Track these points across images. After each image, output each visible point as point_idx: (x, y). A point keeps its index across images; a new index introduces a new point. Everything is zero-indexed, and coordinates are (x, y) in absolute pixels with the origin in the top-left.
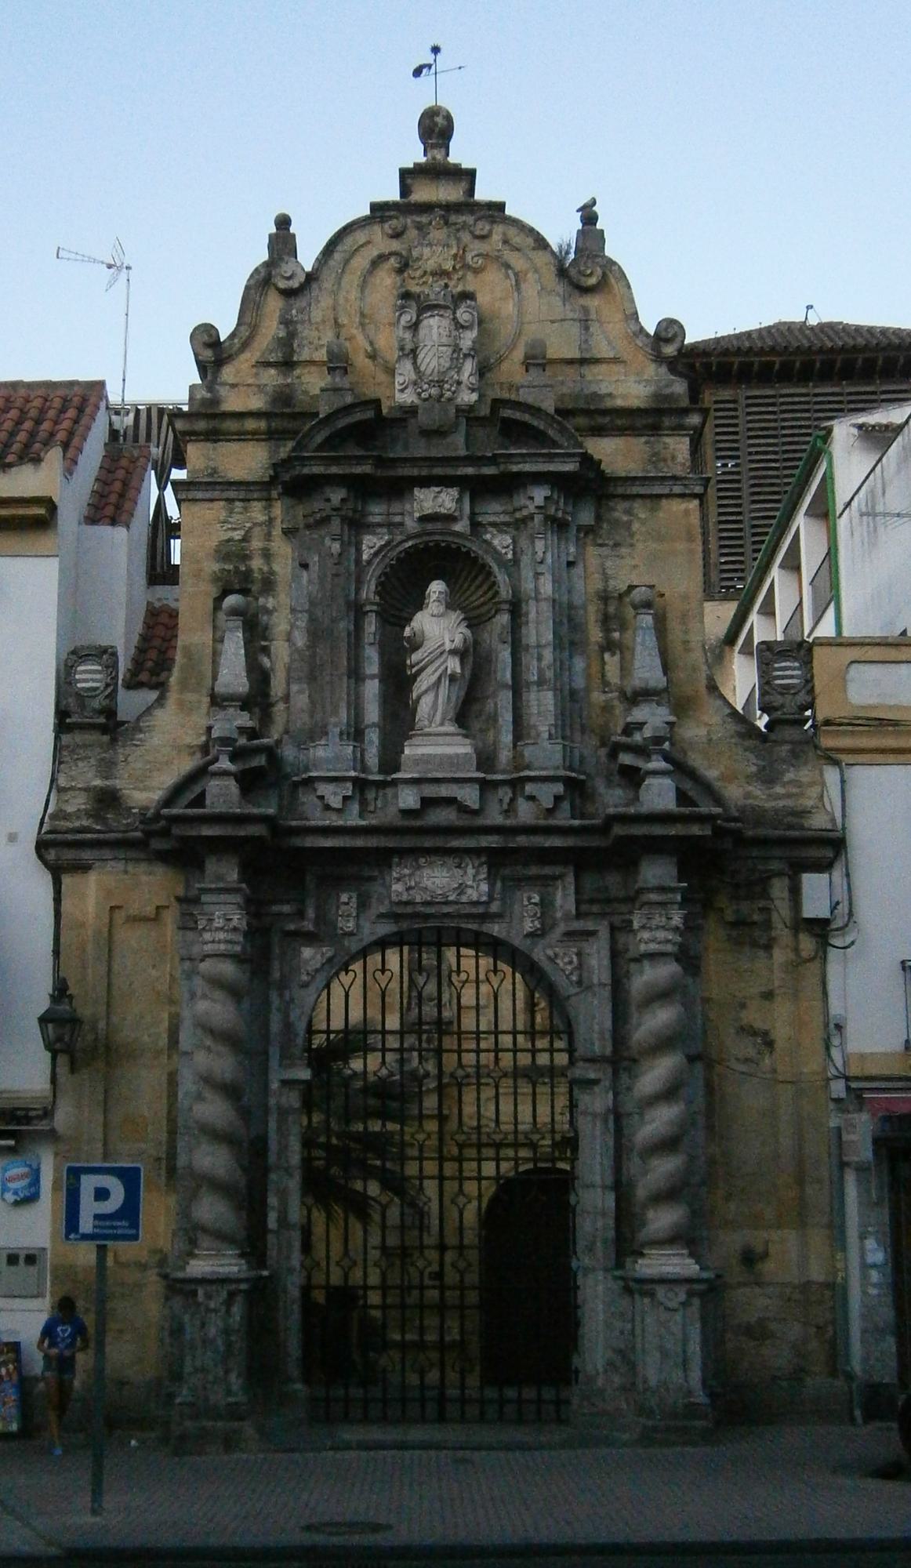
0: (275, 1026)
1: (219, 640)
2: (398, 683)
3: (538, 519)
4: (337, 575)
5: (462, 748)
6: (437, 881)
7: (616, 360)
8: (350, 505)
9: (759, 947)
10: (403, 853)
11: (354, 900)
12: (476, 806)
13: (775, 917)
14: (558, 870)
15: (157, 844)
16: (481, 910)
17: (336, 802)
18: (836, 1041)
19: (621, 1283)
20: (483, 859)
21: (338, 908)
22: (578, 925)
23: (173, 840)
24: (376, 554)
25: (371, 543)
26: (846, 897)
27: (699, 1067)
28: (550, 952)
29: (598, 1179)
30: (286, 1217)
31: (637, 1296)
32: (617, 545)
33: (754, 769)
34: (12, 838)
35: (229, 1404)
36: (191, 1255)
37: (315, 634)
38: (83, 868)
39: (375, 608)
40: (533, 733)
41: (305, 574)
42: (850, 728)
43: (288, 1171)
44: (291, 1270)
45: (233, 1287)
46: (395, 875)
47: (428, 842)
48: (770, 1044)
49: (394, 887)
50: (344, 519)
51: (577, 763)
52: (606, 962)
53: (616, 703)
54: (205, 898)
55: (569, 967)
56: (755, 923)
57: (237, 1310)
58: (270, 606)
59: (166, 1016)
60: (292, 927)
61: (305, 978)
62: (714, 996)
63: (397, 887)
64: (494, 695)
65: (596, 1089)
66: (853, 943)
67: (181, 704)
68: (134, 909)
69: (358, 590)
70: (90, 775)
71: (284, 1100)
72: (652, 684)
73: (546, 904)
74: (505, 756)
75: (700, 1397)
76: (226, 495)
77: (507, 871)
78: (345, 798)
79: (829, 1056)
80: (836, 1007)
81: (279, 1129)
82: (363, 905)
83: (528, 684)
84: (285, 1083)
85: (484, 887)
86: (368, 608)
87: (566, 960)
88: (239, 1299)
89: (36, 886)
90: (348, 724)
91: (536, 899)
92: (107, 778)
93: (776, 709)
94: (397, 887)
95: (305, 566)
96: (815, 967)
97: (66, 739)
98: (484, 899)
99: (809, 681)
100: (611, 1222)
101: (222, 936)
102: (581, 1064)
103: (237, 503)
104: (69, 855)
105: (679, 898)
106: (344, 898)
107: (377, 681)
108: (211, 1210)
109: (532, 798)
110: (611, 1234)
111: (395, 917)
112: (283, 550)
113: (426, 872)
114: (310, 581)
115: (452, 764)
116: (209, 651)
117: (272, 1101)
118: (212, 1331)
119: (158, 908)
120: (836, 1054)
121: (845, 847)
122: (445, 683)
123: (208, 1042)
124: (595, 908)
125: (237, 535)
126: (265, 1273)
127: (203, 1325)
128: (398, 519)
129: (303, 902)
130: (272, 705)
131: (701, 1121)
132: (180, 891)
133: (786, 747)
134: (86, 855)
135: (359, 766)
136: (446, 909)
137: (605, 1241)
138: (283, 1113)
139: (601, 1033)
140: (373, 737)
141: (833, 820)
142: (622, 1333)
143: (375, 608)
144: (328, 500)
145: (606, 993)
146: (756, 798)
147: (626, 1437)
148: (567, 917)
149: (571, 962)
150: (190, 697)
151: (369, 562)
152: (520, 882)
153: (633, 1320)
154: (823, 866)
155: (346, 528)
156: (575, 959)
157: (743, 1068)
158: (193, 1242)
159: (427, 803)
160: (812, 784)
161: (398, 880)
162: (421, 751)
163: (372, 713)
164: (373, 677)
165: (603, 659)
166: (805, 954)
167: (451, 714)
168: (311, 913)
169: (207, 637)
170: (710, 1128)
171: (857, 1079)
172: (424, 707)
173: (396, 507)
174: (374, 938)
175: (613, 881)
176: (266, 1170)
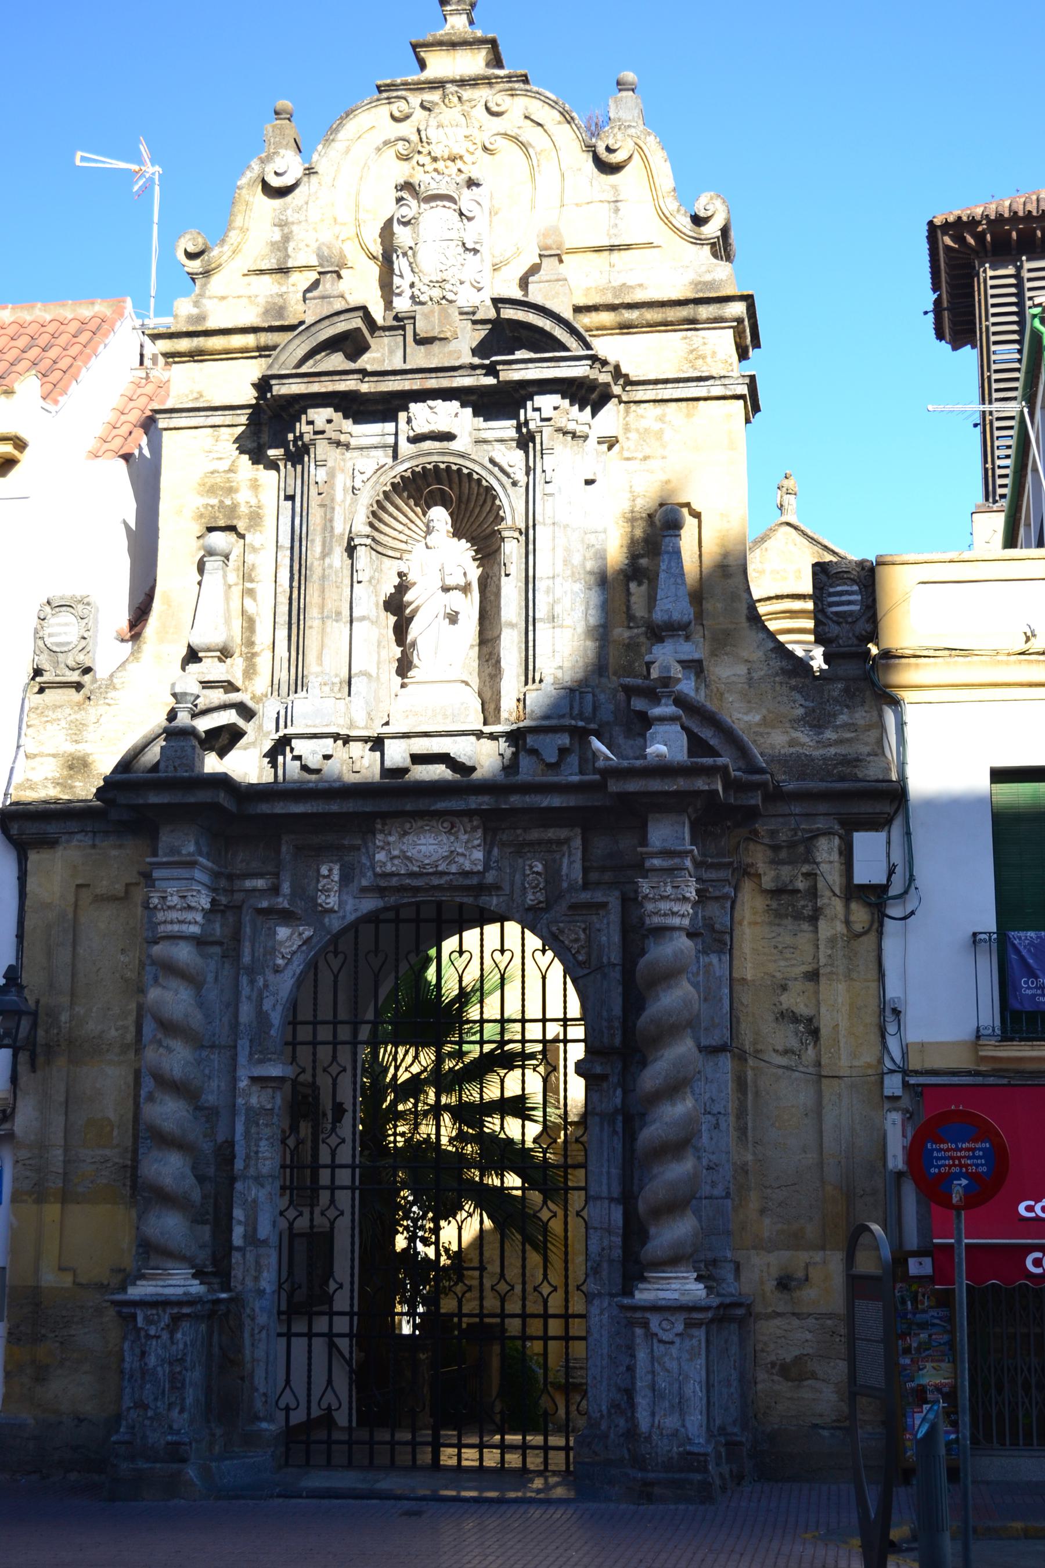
0: (246, 1012)
3: (547, 431)
6: (423, 848)
7: (649, 245)
9: (804, 919)
10: (384, 816)
11: (336, 871)
13: (821, 884)
14: (563, 833)
16: (475, 881)
18: (891, 1028)
20: (475, 823)
21: (318, 881)
22: (585, 896)
27: (726, 1063)
28: (554, 929)
30: (255, 1230)
32: (646, 458)
33: (800, 711)
35: (168, 1443)
38: (49, 843)
43: (258, 1180)
44: (261, 1293)
45: (175, 1311)
48: (815, 1033)
51: (588, 710)
52: (616, 938)
53: (643, 639)
54: (156, 874)
56: (798, 891)
59: (133, 1006)
60: (265, 904)
61: (280, 962)
62: (749, 977)
63: (381, 856)
65: (605, 1085)
66: (912, 913)
68: (103, 887)
71: (254, 1101)
72: (676, 616)
73: (552, 874)
81: (247, 1133)
82: (346, 879)
84: (254, 1079)
85: (478, 855)
87: (573, 936)
91: (539, 867)
96: (870, 940)
98: (480, 868)
100: (618, 1240)
104: (33, 828)
106: (324, 871)
108: (170, 1226)
110: (617, 1253)
113: (410, 838)
117: (240, 1101)
118: (152, 1361)
119: (127, 885)
120: (893, 1044)
124: (607, 877)
127: (143, 1354)
129: (277, 875)
130: (254, 654)
136: (436, 881)
137: (611, 1261)
138: (253, 1115)
145: (616, 974)
146: (803, 745)
149: (577, 940)
152: (521, 849)
154: (877, 823)
156: (582, 936)
157: (783, 1061)
159: (418, 759)
160: (869, 728)
161: (383, 848)
165: (628, 590)
166: (858, 928)
168: (286, 888)
170: (742, 1131)
174: (359, 914)
176: (232, 1180)
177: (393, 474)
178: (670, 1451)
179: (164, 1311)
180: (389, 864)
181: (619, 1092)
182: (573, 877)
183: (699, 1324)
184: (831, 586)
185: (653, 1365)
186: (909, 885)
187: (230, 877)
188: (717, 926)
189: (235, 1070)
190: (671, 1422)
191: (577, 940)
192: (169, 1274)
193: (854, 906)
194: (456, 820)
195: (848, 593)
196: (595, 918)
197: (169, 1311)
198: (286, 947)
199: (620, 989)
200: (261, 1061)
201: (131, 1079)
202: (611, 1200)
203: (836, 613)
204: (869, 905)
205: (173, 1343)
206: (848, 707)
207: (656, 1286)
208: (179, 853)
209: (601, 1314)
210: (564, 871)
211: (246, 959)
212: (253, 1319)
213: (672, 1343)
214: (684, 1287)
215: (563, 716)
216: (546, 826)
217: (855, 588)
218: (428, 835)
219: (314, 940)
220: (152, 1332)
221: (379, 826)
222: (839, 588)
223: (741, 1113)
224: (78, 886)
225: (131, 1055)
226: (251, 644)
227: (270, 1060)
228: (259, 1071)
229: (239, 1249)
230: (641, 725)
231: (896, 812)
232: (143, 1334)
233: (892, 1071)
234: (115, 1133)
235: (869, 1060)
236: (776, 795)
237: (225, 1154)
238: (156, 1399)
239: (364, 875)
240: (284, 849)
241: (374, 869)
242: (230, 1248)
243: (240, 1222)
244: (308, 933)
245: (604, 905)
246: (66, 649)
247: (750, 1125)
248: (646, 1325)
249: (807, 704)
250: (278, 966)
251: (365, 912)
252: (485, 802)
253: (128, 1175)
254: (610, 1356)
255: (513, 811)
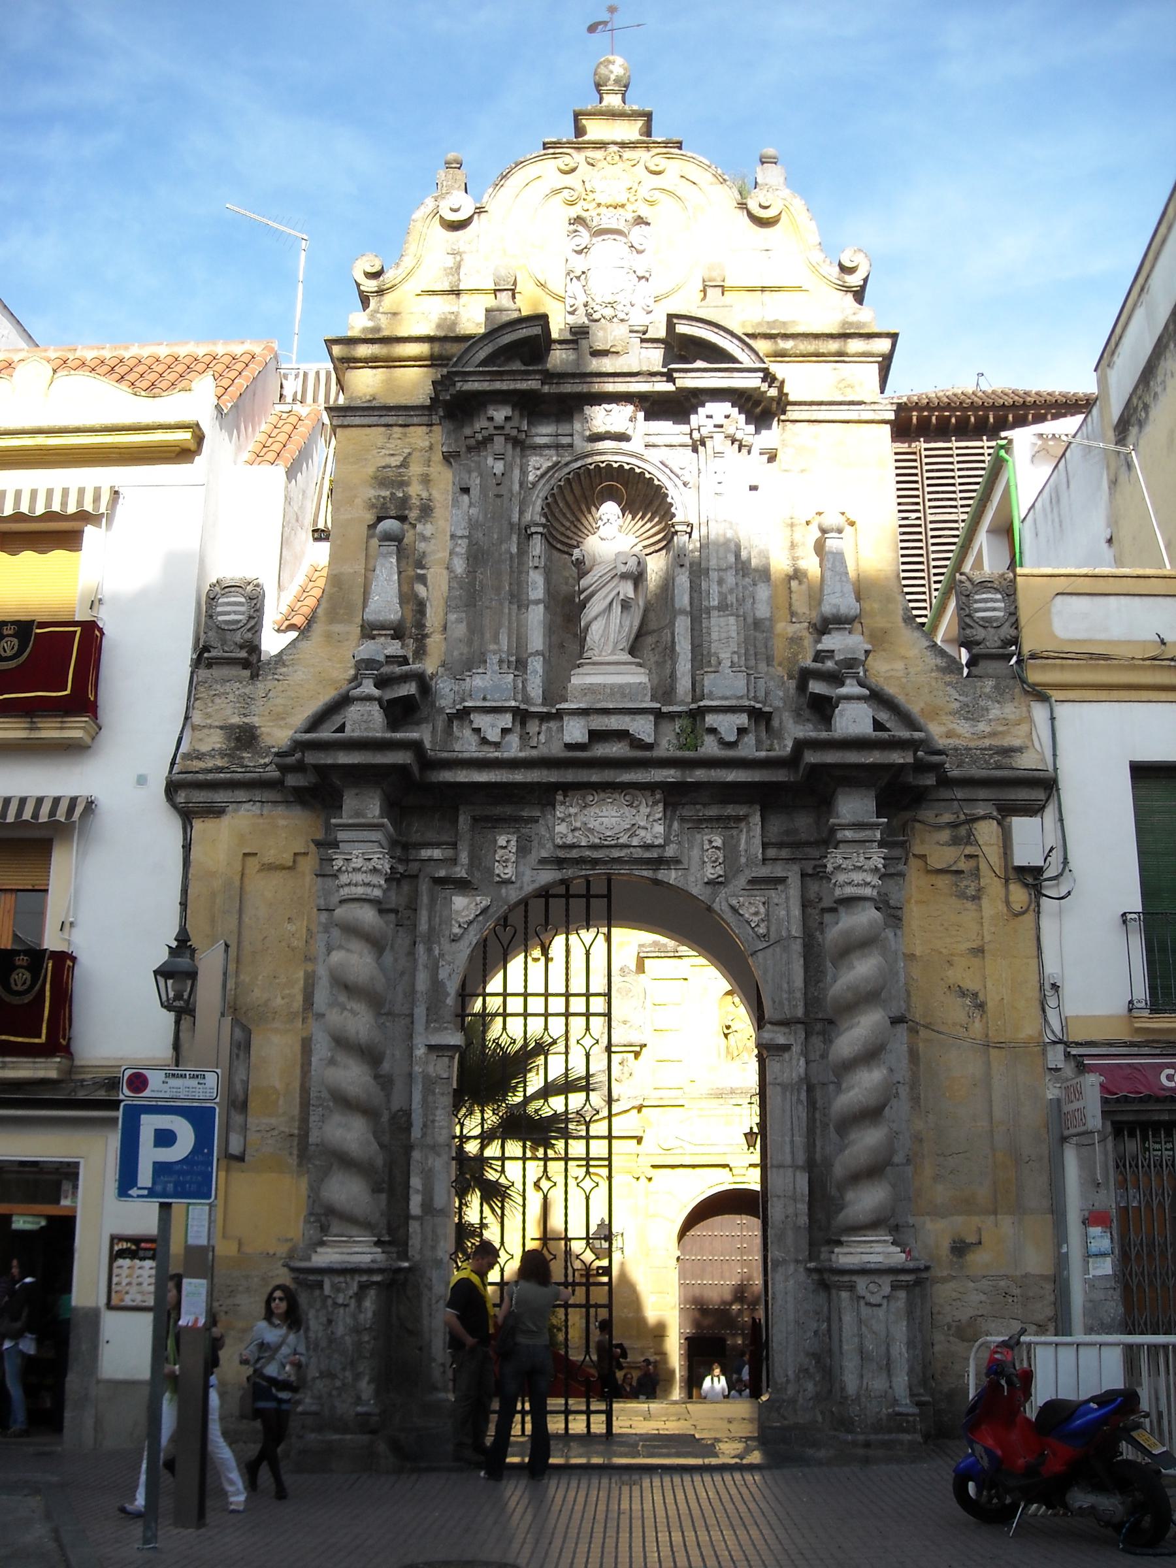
0: (422, 982)
1: (370, 570)
2: (568, 612)
4: (499, 496)
5: (636, 677)
7: (799, 288)
8: (514, 423)
11: (513, 843)
12: (650, 740)
13: (983, 866)
14: (742, 811)
15: (292, 780)
17: (493, 735)
18: (1052, 1002)
19: (815, 1277)
20: (658, 796)
22: (764, 871)
23: (312, 780)
24: (543, 476)
25: (537, 464)
26: (1061, 842)
28: (734, 902)
29: (788, 1160)
30: (432, 1199)
31: (834, 1292)
33: (956, 705)
34: (141, 780)
35: (358, 1414)
36: (322, 1243)
37: (476, 557)
38: (215, 812)
39: (540, 529)
40: (713, 661)
41: (466, 497)
42: (1058, 661)
45: (364, 1278)
46: (558, 814)
47: (595, 777)
48: (981, 1006)
49: (558, 829)
50: (508, 438)
51: (761, 694)
52: (796, 912)
53: (805, 634)
55: (756, 919)
57: (368, 1304)
58: (428, 533)
59: (301, 974)
60: (442, 873)
61: (456, 930)
64: (672, 624)
65: (786, 1056)
66: (1069, 893)
67: (328, 636)
69: (521, 513)
70: (229, 712)
71: (431, 1069)
72: (843, 610)
74: (684, 684)
75: (906, 1405)
76: (384, 420)
77: (687, 812)
78: (505, 731)
79: (1046, 1020)
80: (1051, 968)
81: (424, 1100)
82: (523, 850)
83: (708, 611)
84: (431, 1048)
85: (659, 829)
86: (533, 529)
87: (753, 910)
88: (372, 1293)
89: (169, 830)
90: (509, 654)
91: (718, 842)
92: (245, 715)
93: (978, 643)
94: (561, 828)
95: (466, 490)
96: (1030, 917)
97: (203, 673)
98: (660, 841)
99: (1013, 614)
100: (803, 1207)
101: (359, 877)
102: (768, 1026)
103: (396, 429)
104: (200, 796)
105: (878, 836)
106: (502, 841)
107: (541, 607)
108: (348, 1191)
109: (713, 731)
110: (804, 1220)
111: (560, 863)
112: (444, 479)
113: (592, 811)
114: (471, 505)
115: (624, 695)
116: (361, 580)
117: (417, 1069)
118: (340, 1330)
119: (295, 854)
121: (1058, 790)
122: (617, 608)
123: (342, 998)
124: (785, 853)
125: (395, 461)
126: (406, 1264)
128: (565, 440)
129: (454, 845)
130: (425, 636)
131: (904, 1091)
132: (320, 836)
133: (990, 683)
134: (220, 797)
135: (520, 697)
136: (616, 853)
137: (797, 1228)
138: (430, 1083)
139: (791, 991)
140: (536, 665)
141: (1043, 760)
142: (816, 1333)
143: (540, 529)
144: (491, 419)
145: (797, 947)
147: (822, 1454)
148: (750, 863)
149: (756, 914)
150: (337, 628)
151: (534, 484)
152: (699, 824)
153: (829, 1319)
154: (1033, 810)
155: (510, 446)
156: (762, 910)
158: (324, 1229)
159: (596, 736)
161: (563, 820)
162: (589, 680)
163: (536, 640)
164: (537, 602)
166: (1017, 907)
167: (623, 644)
168: (464, 857)
169: (360, 567)
170: (915, 1100)
171: (1079, 1044)
172: (596, 631)
173: (564, 428)
174: (536, 885)
175: (803, 823)
176: (408, 1148)
177: (567, 470)
178: (878, 1413)
179: (353, 1279)
180: (570, 835)
181: (802, 1061)
182: (753, 851)
183: (900, 1287)
184: (976, 593)
185: (860, 1329)
186: (1064, 869)
187: (406, 847)
188: (892, 903)
189: (411, 1037)
190: (878, 1384)
191: (756, 914)
192: (355, 1242)
193: (1012, 887)
194: (637, 792)
195: (992, 600)
196: (773, 893)
197: (357, 1278)
198: (463, 917)
199: (802, 962)
200: (437, 1030)
201: (298, 1048)
202: (795, 1167)
203: (982, 618)
204: (1026, 885)
205: (361, 1312)
206: (998, 702)
207: (852, 1250)
208: (364, 816)
209: (786, 1280)
210: (743, 846)
211: (423, 927)
212: (430, 1289)
213: (880, 1305)
214: (878, 1251)
215: (741, 697)
216: (725, 801)
217: (999, 596)
218: (610, 807)
219: (491, 910)
220: (340, 1301)
221: (560, 798)
222: (984, 596)
223: (914, 1084)
224: (245, 854)
225: (299, 1024)
226: (420, 625)
227: (446, 1028)
228: (435, 1040)
229: (416, 1218)
230: (823, 709)
231: (1047, 800)
232: (330, 1302)
233: (1054, 1043)
234: (281, 1102)
235: (1030, 1033)
236: (946, 782)
237: (401, 1123)
238: (344, 1369)
239: (544, 847)
240: (461, 819)
241: (553, 840)
242: (408, 1217)
243: (417, 1191)
244: (486, 902)
245: (782, 880)
246: (234, 627)
247: (922, 1096)
248: (852, 1288)
249: (961, 698)
250: (455, 935)
251: (543, 883)
252: (669, 775)
253: (295, 1143)
254: (797, 1322)
255: (698, 786)
